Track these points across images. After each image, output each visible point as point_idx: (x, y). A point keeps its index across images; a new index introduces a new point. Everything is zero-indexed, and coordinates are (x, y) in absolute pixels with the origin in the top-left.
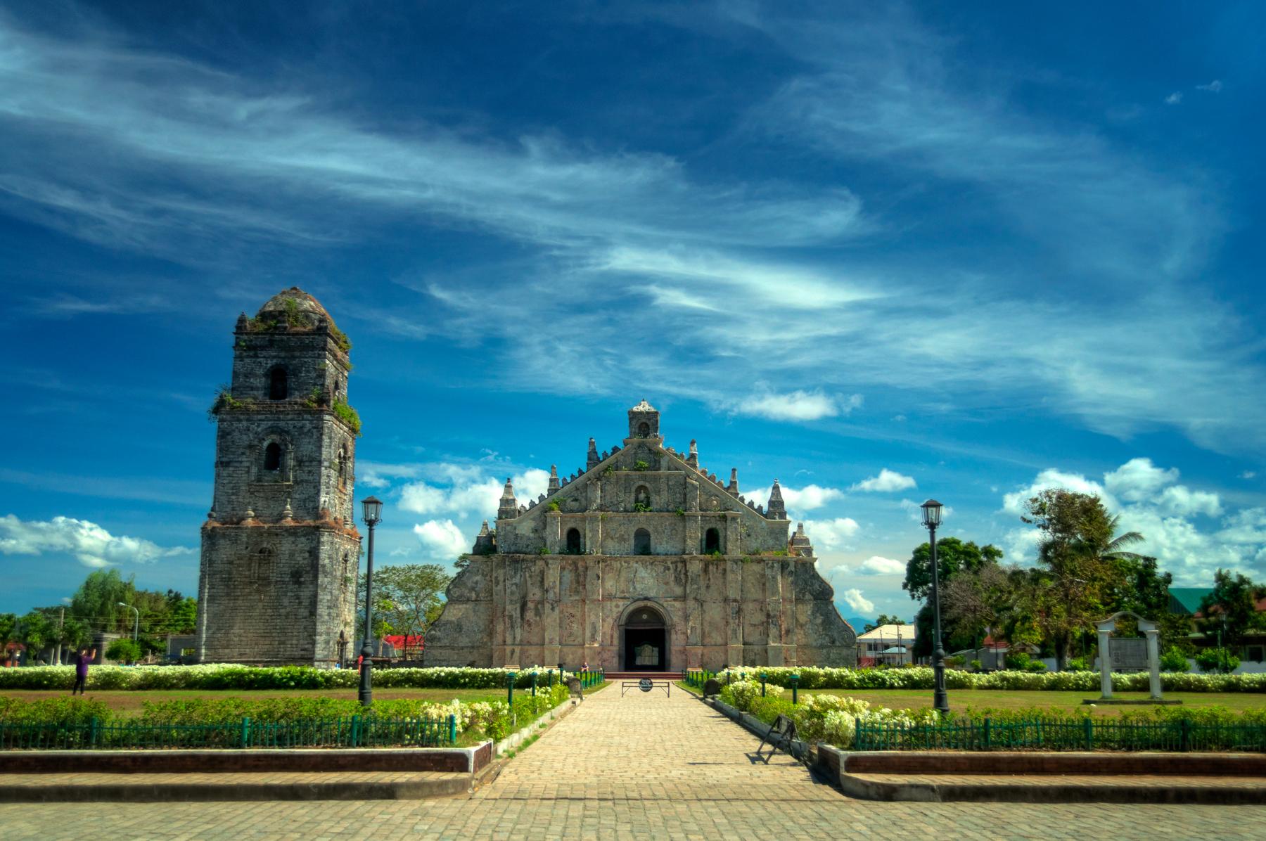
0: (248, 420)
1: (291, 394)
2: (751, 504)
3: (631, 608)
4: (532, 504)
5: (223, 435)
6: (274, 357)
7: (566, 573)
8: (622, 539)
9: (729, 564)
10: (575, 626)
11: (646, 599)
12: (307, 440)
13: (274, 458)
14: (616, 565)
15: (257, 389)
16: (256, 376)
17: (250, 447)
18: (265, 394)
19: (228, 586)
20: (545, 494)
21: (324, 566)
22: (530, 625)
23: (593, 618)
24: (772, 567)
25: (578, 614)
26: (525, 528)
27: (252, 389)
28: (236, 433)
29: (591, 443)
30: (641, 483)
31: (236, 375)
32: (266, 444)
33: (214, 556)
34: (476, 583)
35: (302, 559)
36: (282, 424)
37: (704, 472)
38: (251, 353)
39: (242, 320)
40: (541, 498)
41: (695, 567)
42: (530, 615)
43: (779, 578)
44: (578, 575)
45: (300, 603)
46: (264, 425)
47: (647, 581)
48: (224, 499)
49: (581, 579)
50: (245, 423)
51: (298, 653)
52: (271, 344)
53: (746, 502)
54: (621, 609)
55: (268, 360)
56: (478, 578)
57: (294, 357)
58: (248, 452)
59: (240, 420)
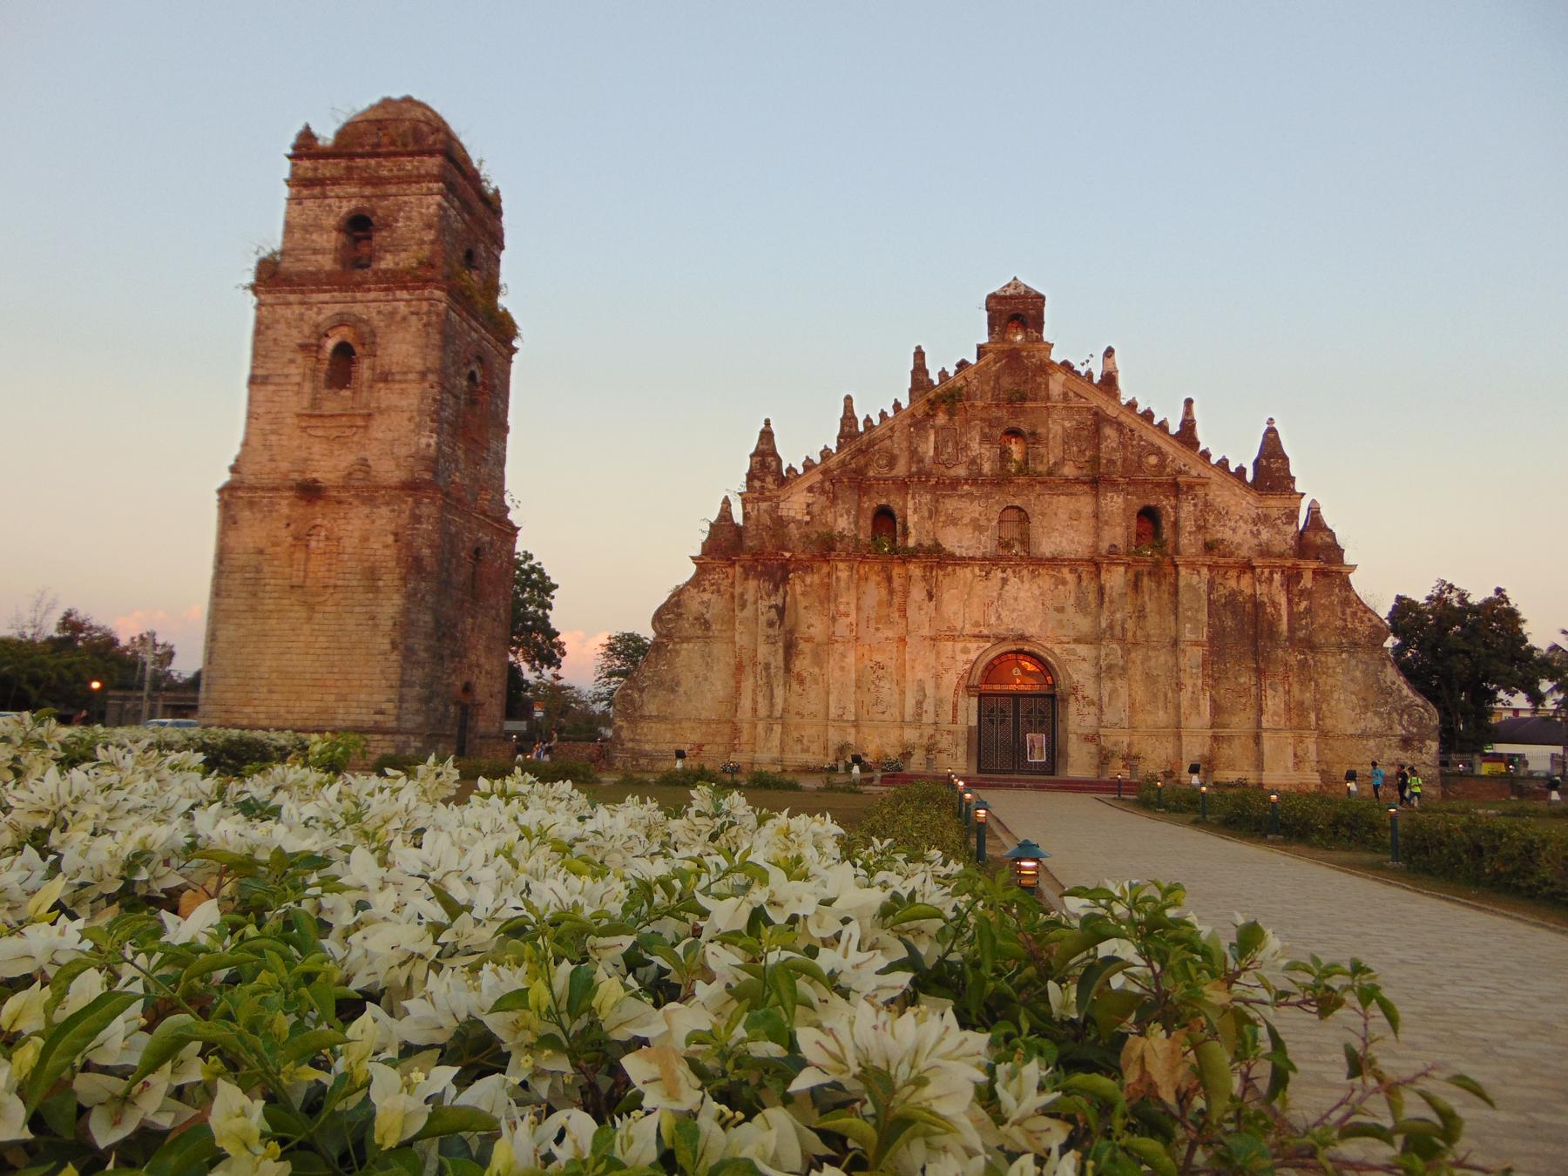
0: (302, 303)
1: (381, 259)
2: (1223, 464)
3: (993, 654)
4: (809, 465)
5: (260, 329)
6: (349, 197)
7: (872, 584)
8: (977, 527)
9: (1183, 571)
10: (885, 684)
11: (1022, 638)
12: (400, 335)
13: (343, 366)
14: (965, 574)
15: (322, 252)
16: (320, 228)
17: (304, 347)
18: (335, 260)
19: (255, 595)
20: (833, 447)
21: (418, 560)
22: (801, 682)
23: (920, 675)
24: (1271, 580)
25: (892, 666)
26: (795, 505)
27: (315, 252)
28: (282, 326)
29: (919, 354)
30: (1013, 424)
31: (289, 228)
32: (330, 344)
33: (232, 540)
34: (707, 604)
35: (382, 549)
36: (358, 309)
37: (1132, 405)
38: (317, 190)
39: (307, 137)
40: (825, 454)
41: (1116, 579)
42: (802, 664)
43: (1282, 600)
44: (891, 592)
45: (377, 625)
46: (330, 311)
47: (1026, 607)
48: (256, 442)
49: (897, 600)
50: (297, 309)
51: (368, 718)
52: (348, 176)
53: (1214, 460)
54: (973, 656)
55: (345, 199)
56: (706, 596)
57: (385, 197)
58: (299, 358)
59: (288, 304)
